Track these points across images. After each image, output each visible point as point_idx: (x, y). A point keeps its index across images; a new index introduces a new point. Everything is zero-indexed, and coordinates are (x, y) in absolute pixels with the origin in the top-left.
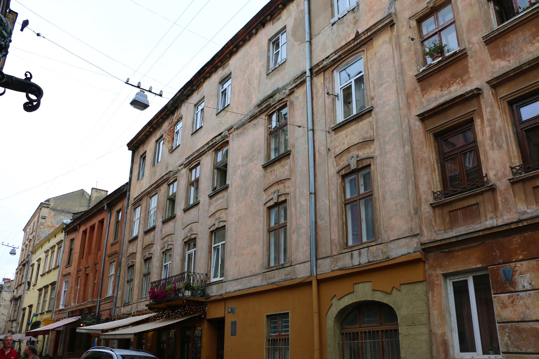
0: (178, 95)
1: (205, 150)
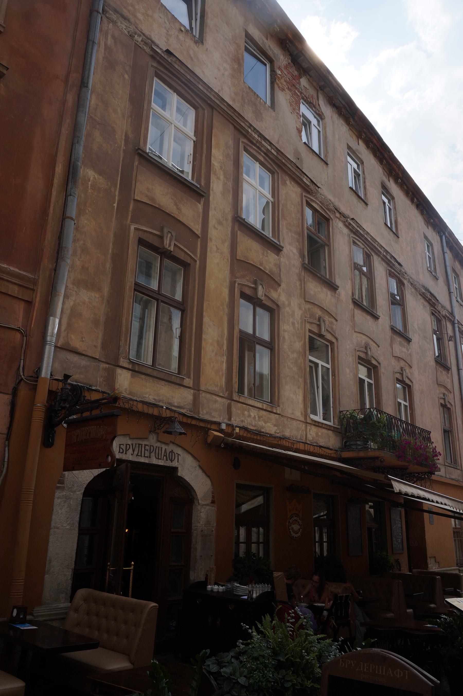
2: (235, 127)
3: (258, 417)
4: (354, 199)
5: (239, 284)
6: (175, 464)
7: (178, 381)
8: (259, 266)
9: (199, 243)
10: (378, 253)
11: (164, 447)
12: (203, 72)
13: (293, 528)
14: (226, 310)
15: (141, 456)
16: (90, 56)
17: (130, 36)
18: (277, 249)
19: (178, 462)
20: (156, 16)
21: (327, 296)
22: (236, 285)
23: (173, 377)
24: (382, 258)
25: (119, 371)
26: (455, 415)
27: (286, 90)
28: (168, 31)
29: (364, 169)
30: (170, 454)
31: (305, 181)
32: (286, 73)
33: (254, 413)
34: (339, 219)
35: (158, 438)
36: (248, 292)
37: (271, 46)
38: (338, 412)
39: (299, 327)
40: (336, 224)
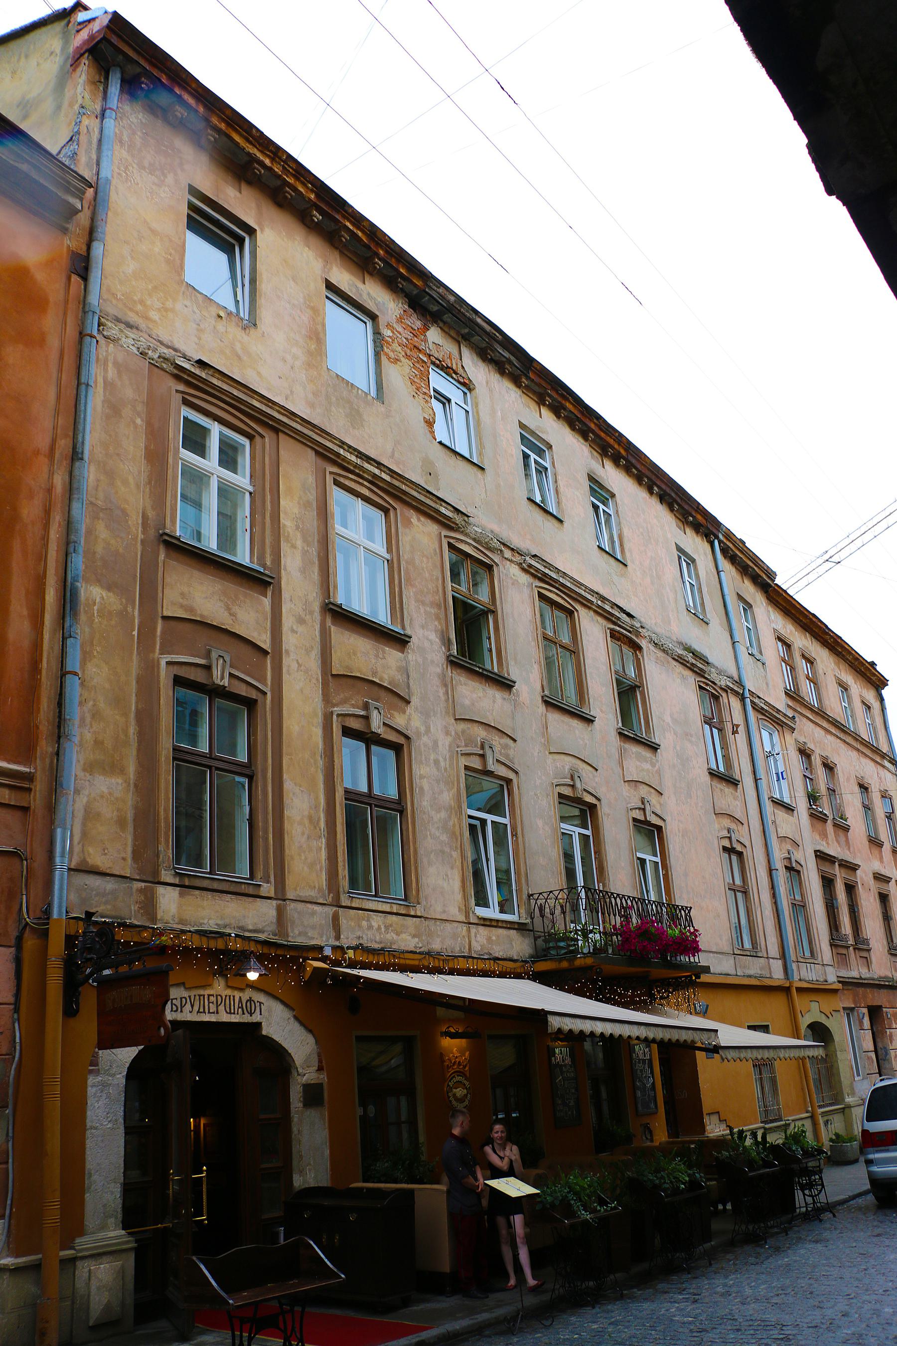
0: (479, 320)
1: (591, 602)
2: (317, 453)
3: (385, 926)
4: (538, 515)
5: (338, 715)
6: (256, 1018)
7: (251, 891)
8: (371, 678)
9: (269, 661)
10: (587, 604)
11: (237, 994)
12: (259, 373)
13: (454, 1095)
14: (321, 763)
15: (204, 1012)
16: (83, 408)
17: (141, 354)
18: (400, 641)
19: (261, 1014)
20: (179, 306)
21: (494, 702)
22: (335, 717)
23: (243, 886)
24: (595, 612)
25: (161, 890)
26: (751, 863)
27: (403, 359)
28: (198, 325)
29: (553, 458)
30: (248, 1004)
31: (444, 512)
32: (400, 330)
33: (377, 921)
34: (511, 561)
35: (227, 982)
36: (355, 724)
37: (371, 292)
38: (525, 897)
39: (448, 766)
40: (504, 571)
